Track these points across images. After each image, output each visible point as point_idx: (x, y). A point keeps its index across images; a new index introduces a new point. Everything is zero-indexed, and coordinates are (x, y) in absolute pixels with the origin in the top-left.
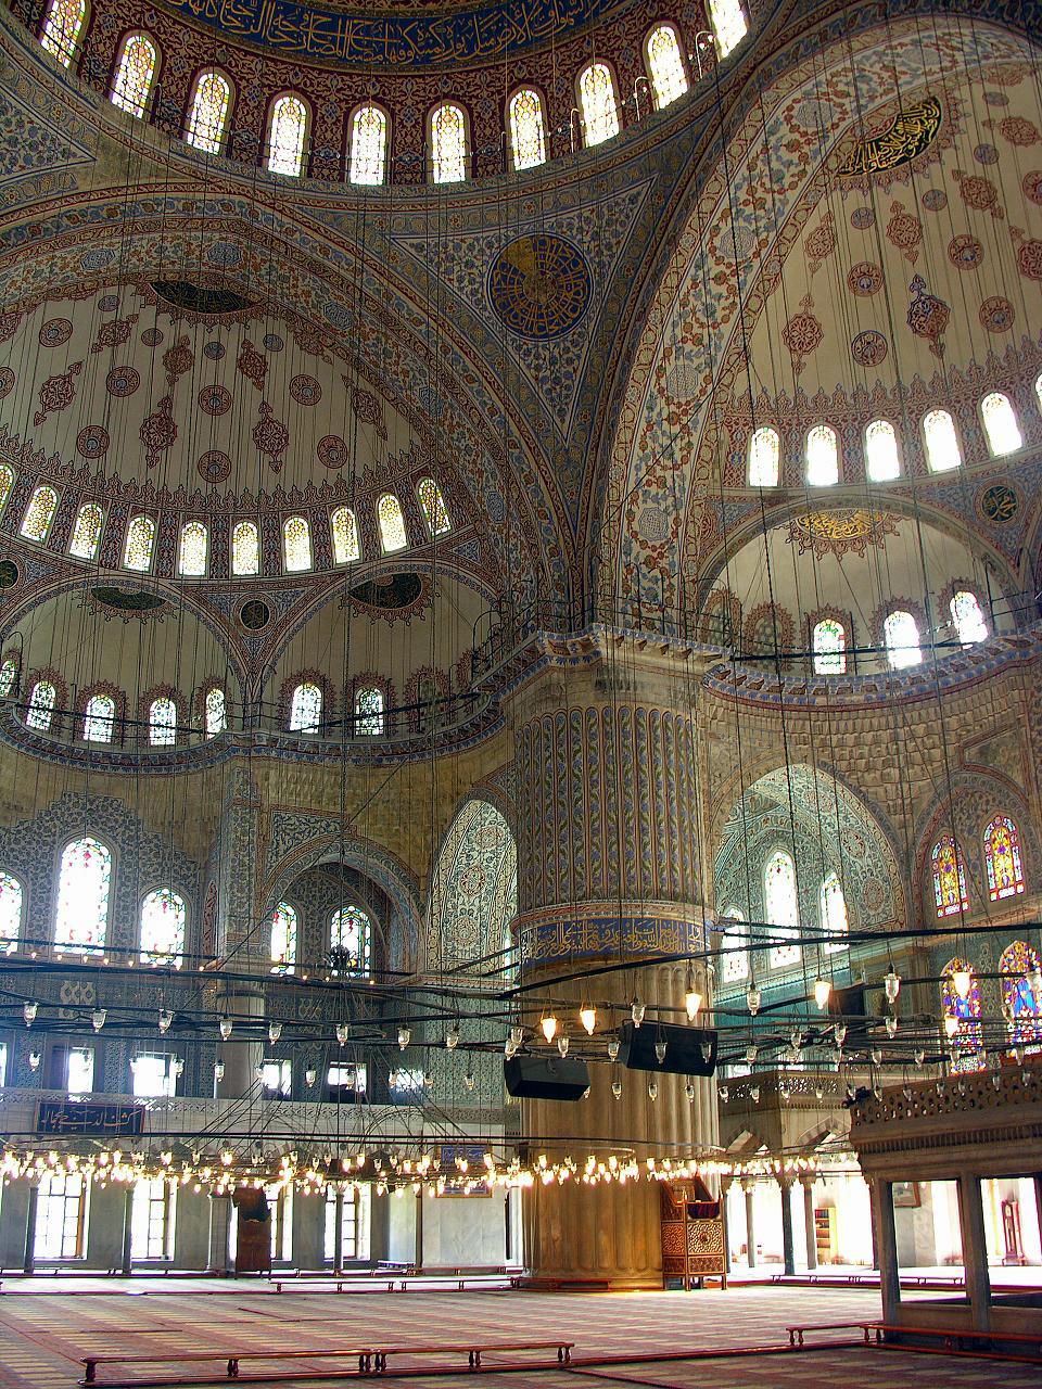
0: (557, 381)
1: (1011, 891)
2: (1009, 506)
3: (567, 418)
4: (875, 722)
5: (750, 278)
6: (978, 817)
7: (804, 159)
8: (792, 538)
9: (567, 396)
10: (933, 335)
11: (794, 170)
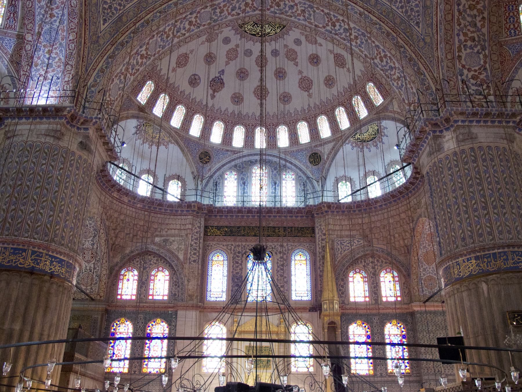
0: (110, 7)
1: (160, 298)
2: (207, 160)
3: (106, 25)
4: (128, 212)
5: (196, 30)
6: (151, 264)
7: (244, 11)
8: (136, 127)
9: (111, 17)
10: (214, 91)
11: (239, 11)
